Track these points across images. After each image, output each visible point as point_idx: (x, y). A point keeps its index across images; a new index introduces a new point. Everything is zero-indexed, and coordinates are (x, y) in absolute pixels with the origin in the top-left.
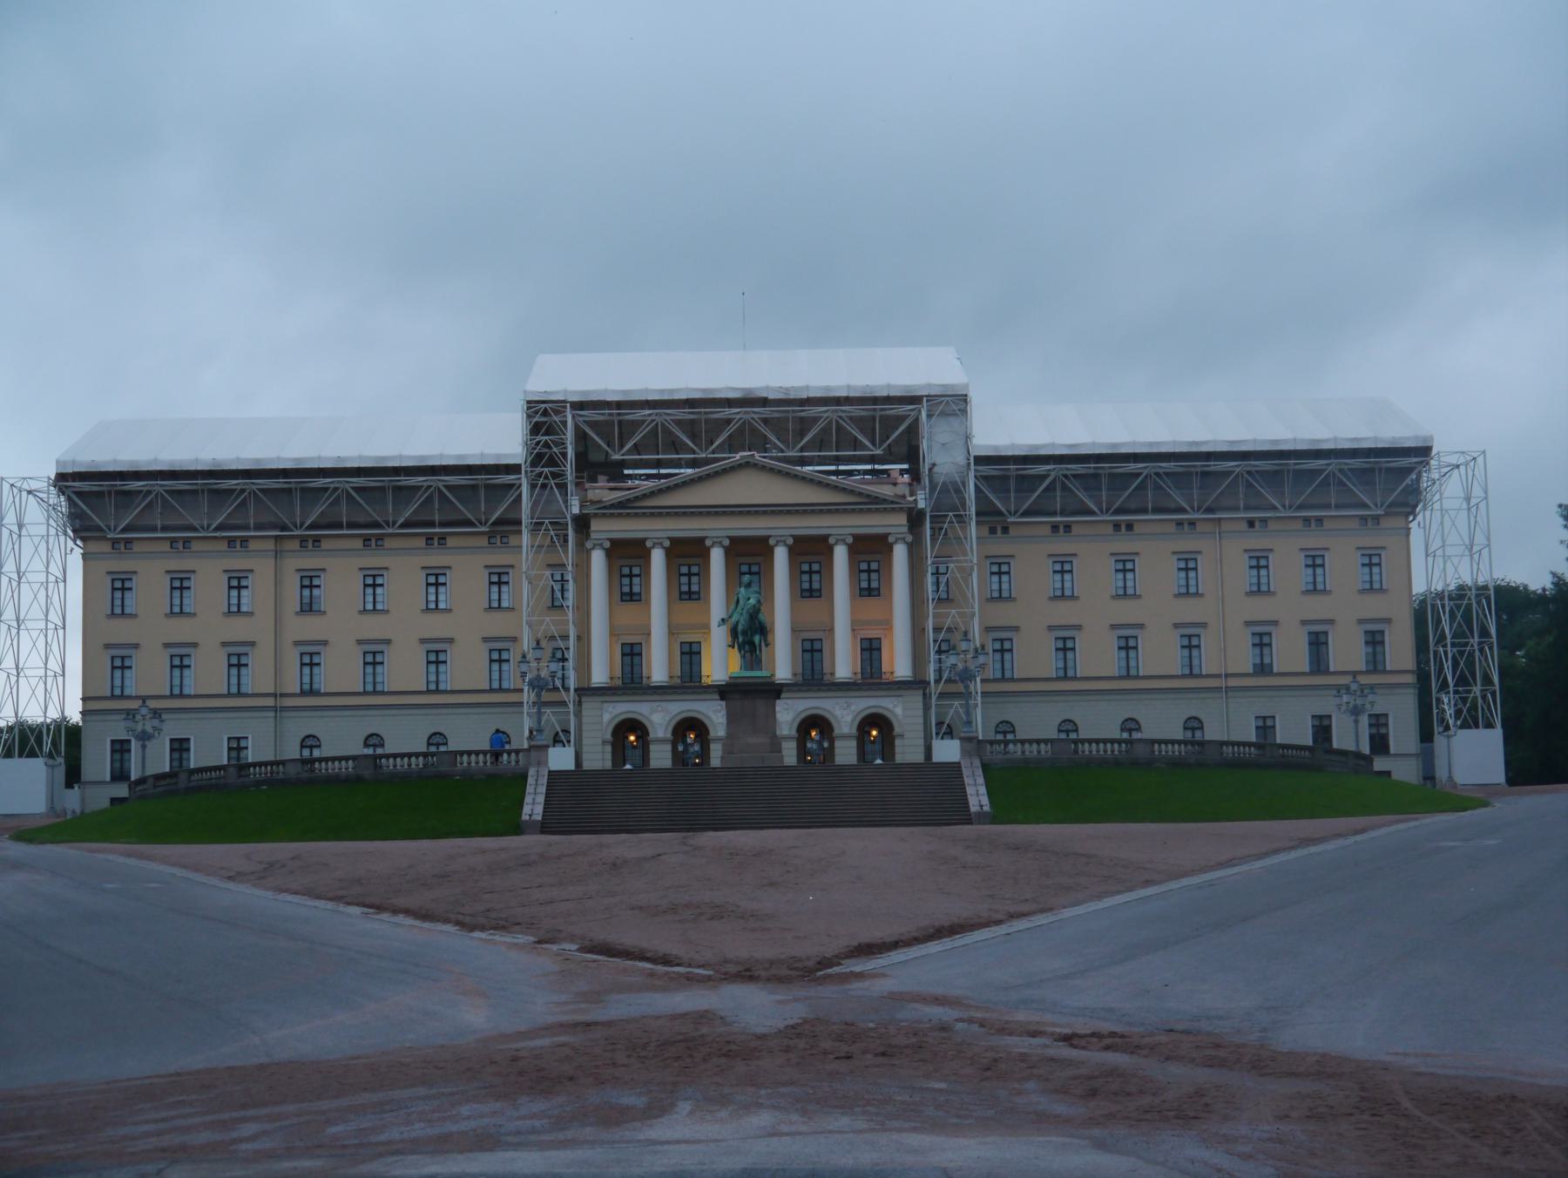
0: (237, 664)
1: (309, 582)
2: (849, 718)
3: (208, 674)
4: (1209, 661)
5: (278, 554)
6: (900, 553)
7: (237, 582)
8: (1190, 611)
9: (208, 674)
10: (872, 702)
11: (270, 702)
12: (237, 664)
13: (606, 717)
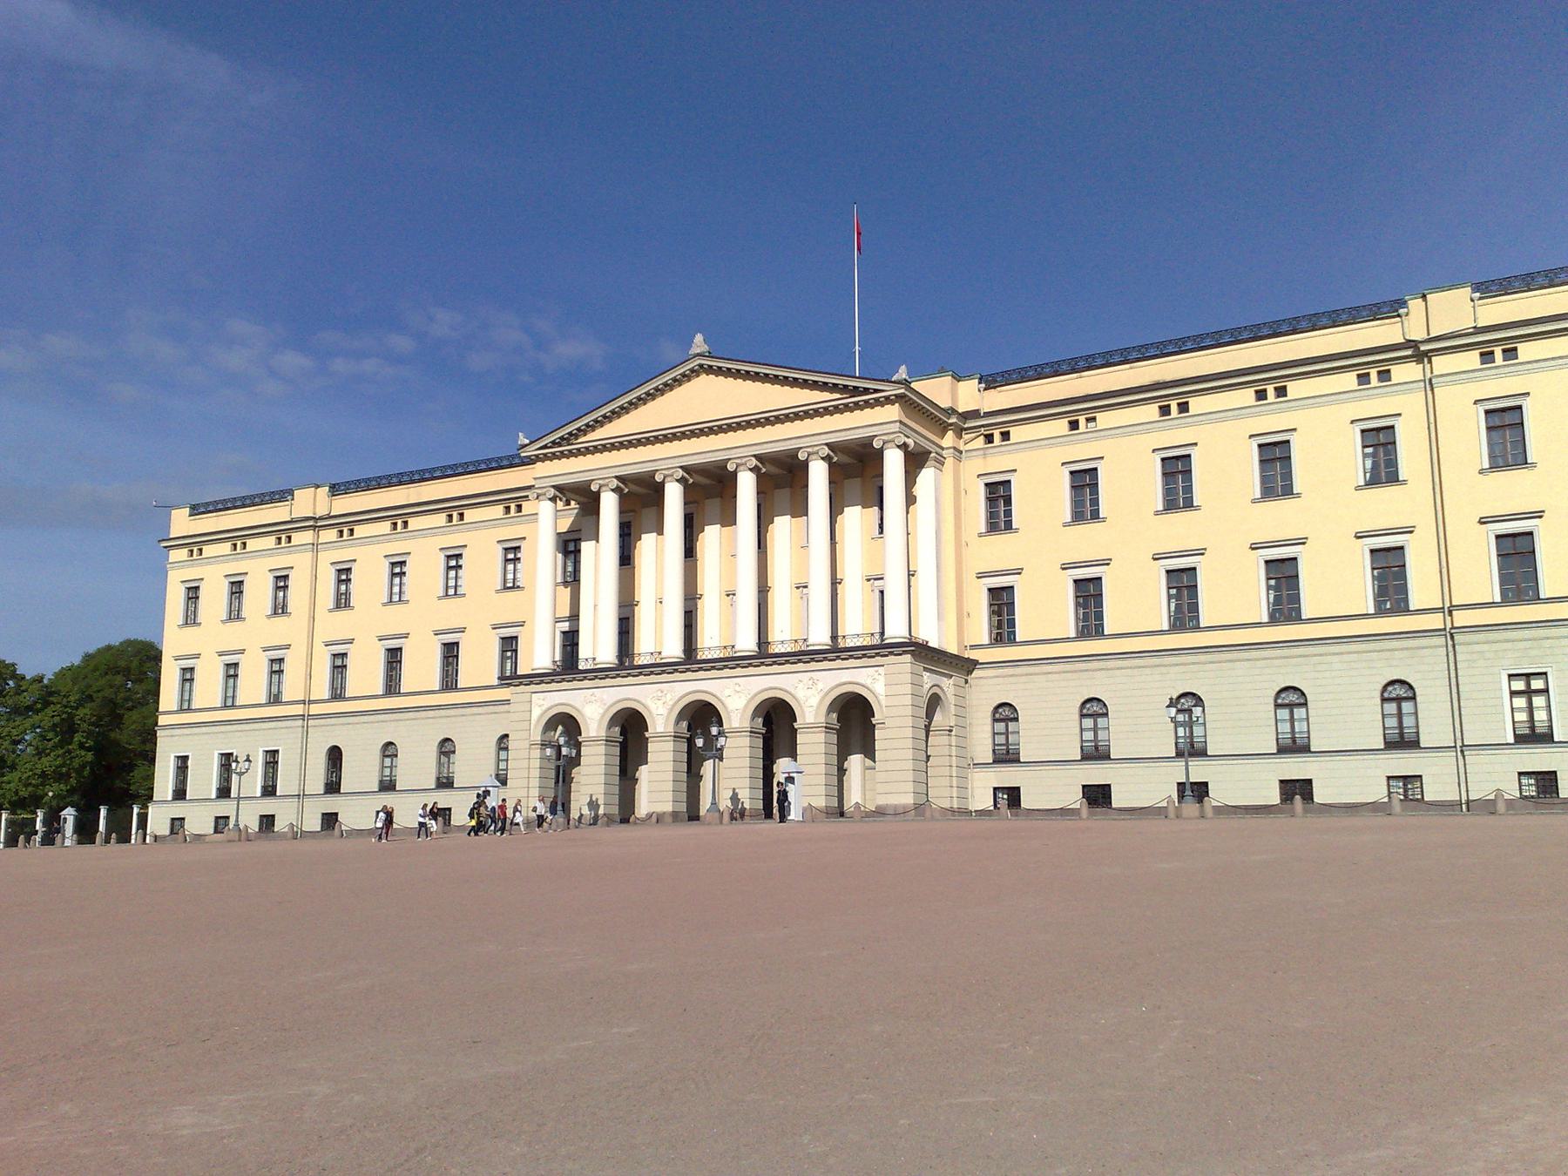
0: (276, 668)
1: (344, 574)
2: (814, 701)
3: (253, 685)
4: (1422, 588)
5: (315, 547)
6: (894, 462)
7: (281, 582)
8: (1385, 508)
9: (253, 685)
10: (845, 676)
11: (298, 710)
12: (276, 668)
13: (536, 712)
